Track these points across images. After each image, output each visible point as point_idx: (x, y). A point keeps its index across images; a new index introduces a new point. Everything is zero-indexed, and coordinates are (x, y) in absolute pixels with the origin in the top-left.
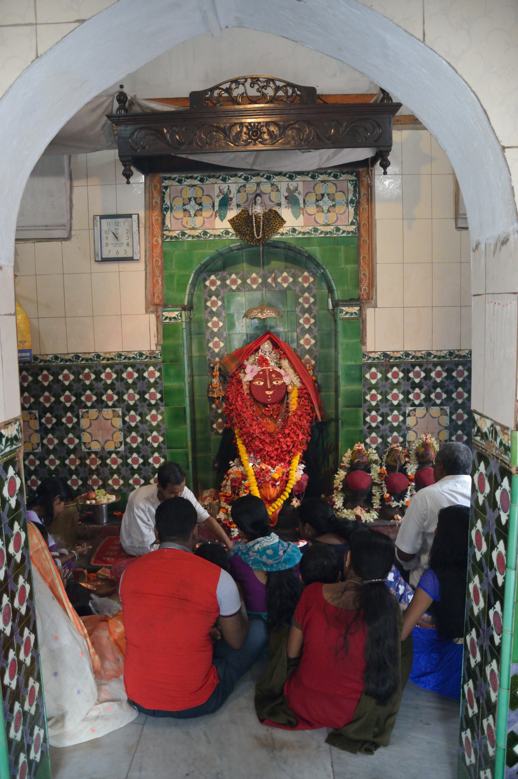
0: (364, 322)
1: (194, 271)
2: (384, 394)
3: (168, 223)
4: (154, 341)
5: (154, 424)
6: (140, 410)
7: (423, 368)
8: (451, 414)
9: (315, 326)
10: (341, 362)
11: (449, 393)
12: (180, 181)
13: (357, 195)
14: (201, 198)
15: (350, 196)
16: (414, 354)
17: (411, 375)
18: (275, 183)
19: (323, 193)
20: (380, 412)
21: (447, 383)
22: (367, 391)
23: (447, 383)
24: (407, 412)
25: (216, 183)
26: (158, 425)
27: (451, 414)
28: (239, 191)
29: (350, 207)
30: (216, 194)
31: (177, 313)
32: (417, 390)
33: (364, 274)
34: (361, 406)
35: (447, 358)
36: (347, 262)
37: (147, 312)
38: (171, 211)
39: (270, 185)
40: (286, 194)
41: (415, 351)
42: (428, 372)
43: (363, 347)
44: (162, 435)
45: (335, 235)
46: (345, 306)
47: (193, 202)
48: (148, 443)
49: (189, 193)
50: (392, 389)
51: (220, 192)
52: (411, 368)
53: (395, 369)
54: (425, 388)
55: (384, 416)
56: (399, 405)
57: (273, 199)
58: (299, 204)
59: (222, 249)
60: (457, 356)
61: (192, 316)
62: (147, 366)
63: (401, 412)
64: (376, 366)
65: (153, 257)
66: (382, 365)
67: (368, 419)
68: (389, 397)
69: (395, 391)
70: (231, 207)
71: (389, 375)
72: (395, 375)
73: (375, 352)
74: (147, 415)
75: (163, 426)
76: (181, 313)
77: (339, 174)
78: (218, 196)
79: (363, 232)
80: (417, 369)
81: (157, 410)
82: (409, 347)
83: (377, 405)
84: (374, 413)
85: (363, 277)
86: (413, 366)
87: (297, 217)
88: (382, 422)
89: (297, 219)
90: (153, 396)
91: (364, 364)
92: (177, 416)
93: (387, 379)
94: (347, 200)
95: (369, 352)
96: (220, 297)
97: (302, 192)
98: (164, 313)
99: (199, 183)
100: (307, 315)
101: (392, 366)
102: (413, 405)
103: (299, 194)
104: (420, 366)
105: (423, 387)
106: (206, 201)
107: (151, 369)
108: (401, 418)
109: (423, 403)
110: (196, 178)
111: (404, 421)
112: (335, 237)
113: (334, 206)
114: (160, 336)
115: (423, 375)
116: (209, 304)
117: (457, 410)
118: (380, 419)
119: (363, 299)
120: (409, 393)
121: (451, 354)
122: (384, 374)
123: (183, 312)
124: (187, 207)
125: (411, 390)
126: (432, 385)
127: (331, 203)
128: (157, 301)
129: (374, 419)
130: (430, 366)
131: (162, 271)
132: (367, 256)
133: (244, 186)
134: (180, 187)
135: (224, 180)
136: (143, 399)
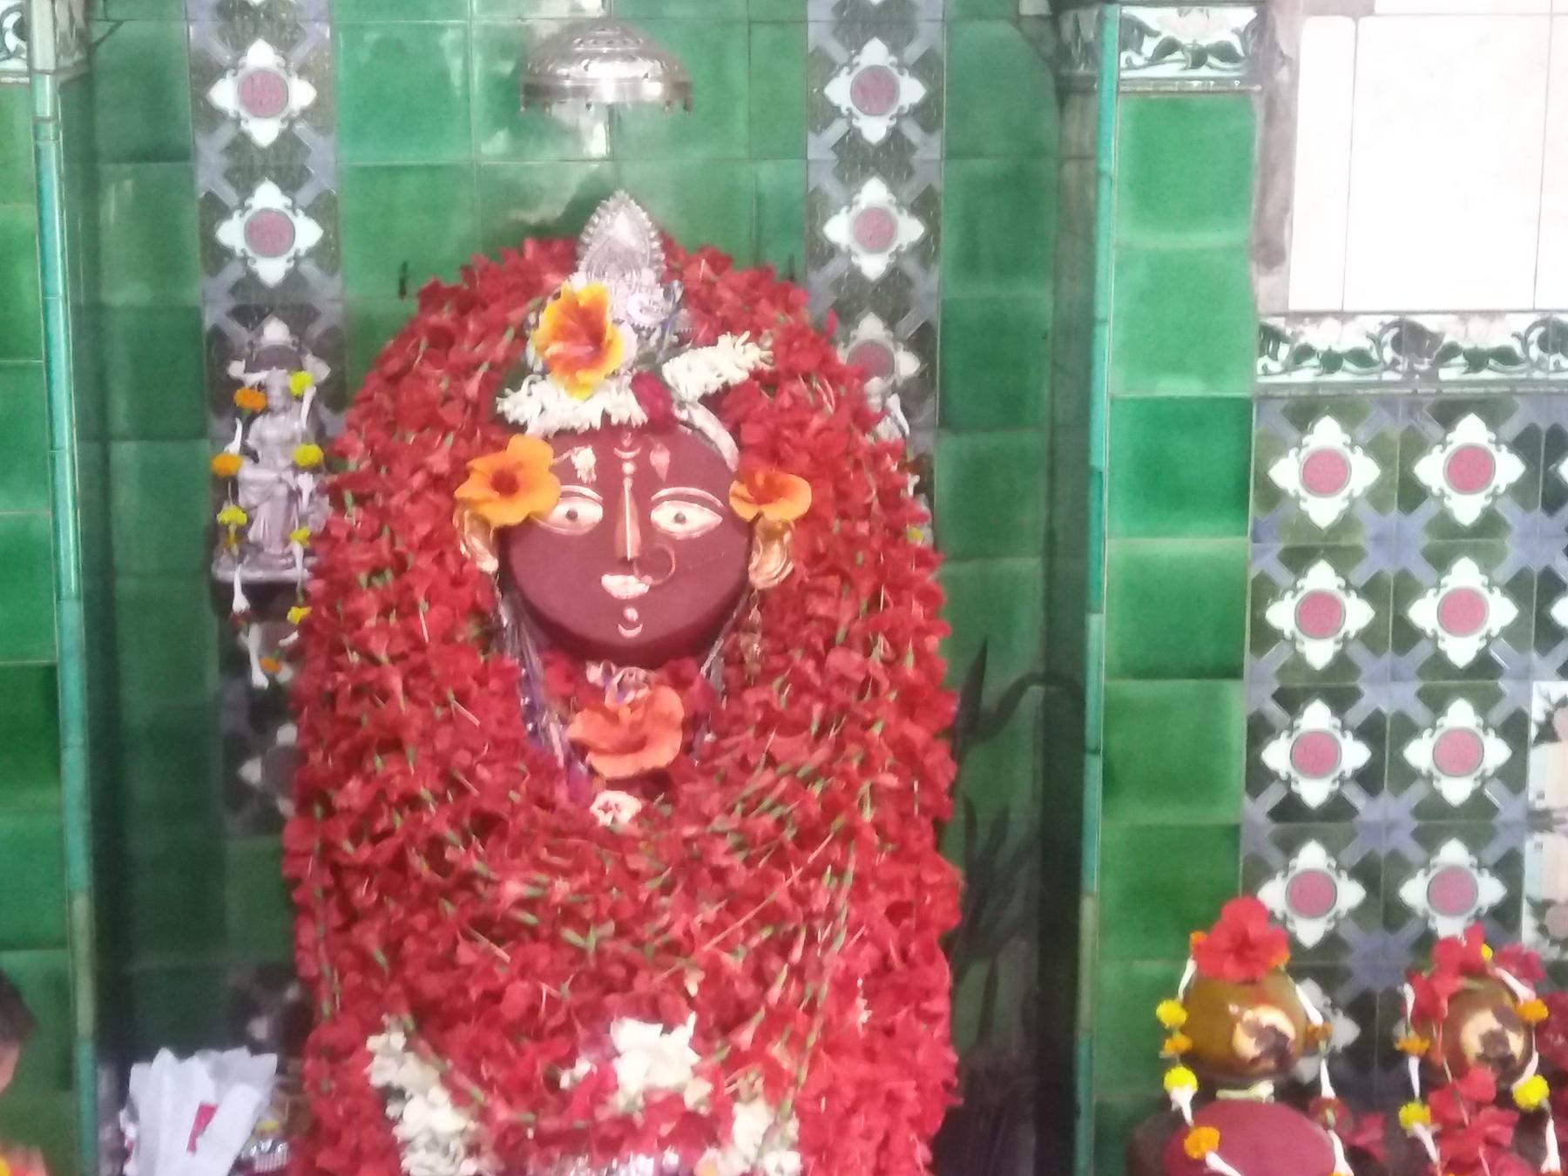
0: (1278, 111)
9: (928, 127)
10: (1113, 379)
20: (1357, 714)
22: (1281, 574)
24: (1537, 713)
34: (1235, 672)
43: (1264, 284)
50: (1440, 561)
53: (1471, 430)
56: (1484, 666)
63: (1499, 714)
64: (1347, 408)
66: (1387, 403)
67: (1277, 755)
69: (1465, 573)
71: (1431, 470)
72: (1470, 470)
73: (1342, 316)
83: (1342, 664)
84: (1317, 716)
88: (1368, 779)
91: (1266, 397)
93: (1411, 494)
95: (1300, 316)
101: (1448, 412)
108: (1496, 752)
111: (1514, 775)
118: (1355, 754)
129: (1315, 756)
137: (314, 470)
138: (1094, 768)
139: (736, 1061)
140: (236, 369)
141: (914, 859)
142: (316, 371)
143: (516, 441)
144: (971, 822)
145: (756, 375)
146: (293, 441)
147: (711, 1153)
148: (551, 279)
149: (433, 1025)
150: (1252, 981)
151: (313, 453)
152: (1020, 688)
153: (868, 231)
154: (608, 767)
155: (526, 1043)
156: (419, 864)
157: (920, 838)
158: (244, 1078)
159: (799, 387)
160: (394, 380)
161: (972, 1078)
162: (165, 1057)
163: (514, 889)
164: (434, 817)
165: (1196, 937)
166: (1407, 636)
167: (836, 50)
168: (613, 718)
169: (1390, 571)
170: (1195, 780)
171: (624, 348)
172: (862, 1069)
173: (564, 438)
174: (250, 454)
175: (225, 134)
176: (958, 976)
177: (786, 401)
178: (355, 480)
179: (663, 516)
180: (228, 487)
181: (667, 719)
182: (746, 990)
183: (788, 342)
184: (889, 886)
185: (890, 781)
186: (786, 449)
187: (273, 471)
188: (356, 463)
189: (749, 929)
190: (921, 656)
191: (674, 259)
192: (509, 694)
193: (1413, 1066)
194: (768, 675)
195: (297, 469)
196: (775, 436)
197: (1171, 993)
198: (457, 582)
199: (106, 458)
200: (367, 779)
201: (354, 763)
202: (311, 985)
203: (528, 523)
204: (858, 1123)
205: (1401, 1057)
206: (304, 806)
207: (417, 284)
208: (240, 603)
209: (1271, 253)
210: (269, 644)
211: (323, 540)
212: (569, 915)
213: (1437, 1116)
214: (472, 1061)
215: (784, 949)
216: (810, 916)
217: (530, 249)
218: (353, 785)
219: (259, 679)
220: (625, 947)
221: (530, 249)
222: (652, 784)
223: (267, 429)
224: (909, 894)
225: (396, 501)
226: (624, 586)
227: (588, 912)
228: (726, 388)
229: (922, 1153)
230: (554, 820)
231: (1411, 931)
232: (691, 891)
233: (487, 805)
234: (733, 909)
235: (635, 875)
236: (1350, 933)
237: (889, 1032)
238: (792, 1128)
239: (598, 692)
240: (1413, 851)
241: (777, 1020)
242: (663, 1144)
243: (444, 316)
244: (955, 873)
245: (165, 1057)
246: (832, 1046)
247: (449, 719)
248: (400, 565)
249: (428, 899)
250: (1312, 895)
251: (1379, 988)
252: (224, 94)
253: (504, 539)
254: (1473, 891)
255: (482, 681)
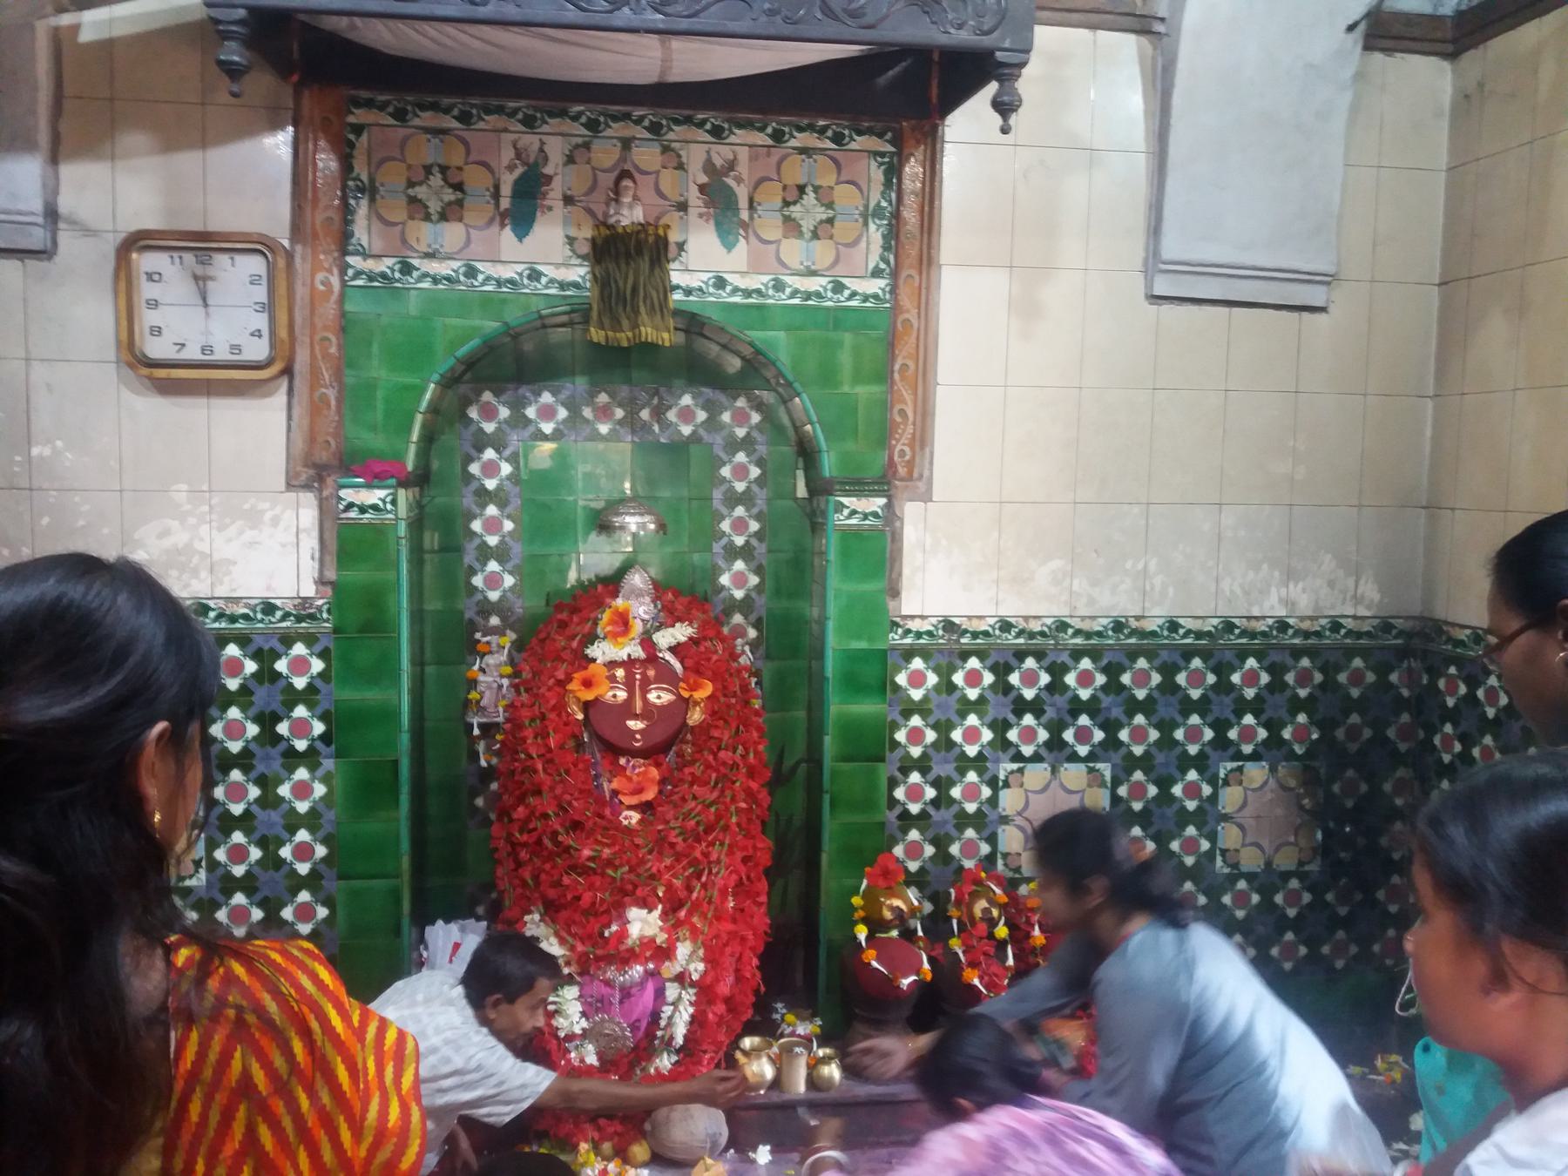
0: (897, 537)
1: (436, 377)
2: (943, 728)
3: (361, 232)
4: (310, 569)
5: (302, 807)
6: (261, 768)
7: (1046, 662)
8: (1116, 782)
10: (833, 641)
11: (1111, 727)
12: (401, 115)
13: (893, 195)
14: (460, 169)
15: (875, 197)
16: (1022, 624)
17: (1014, 679)
18: (674, 145)
19: (801, 181)
20: (932, 776)
21: (1106, 701)
22: (900, 719)
23: (1106, 701)
24: (1002, 777)
25: (506, 130)
26: (313, 812)
27: (1116, 782)
28: (570, 160)
29: (872, 227)
30: (505, 161)
31: (382, 493)
32: (1028, 719)
33: (902, 412)
34: (882, 760)
35: (1108, 637)
36: (858, 378)
37: (290, 486)
38: (372, 200)
39: (658, 150)
40: (703, 179)
41: (1026, 618)
42: (1057, 671)
43: (892, 604)
44: (325, 841)
45: (830, 304)
46: (848, 494)
47: (436, 180)
48: (280, 863)
49: (428, 151)
50: (963, 715)
51: (518, 155)
52: (1013, 662)
53: (973, 663)
54: (1050, 713)
55: (942, 785)
56: (980, 756)
57: (665, 187)
58: (736, 210)
59: (514, 316)
60: (1134, 632)
61: (425, 501)
62: (288, 640)
63: (987, 776)
64: (925, 653)
65: (313, 326)
66: (941, 651)
67: (899, 793)
68: (957, 735)
69: (972, 720)
70: (547, 202)
71: (958, 678)
72: (973, 678)
73: (923, 617)
74: (281, 782)
75: (330, 815)
76: (395, 496)
77: (846, 132)
78: (511, 168)
79: (906, 301)
80: (1030, 663)
81: (313, 768)
82: (1013, 607)
83: (924, 755)
84: (915, 777)
85: (898, 419)
86: (1020, 655)
87: (729, 246)
88: (935, 803)
89: (729, 251)
90: (301, 728)
91: (894, 648)
92: (369, 787)
93: (952, 688)
94: (866, 207)
96: (507, 452)
97: (745, 176)
98: (342, 493)
99: (455, 124)
100: (740, 511)
101: (965, 655)
102: (1018, 757)
103: (739, 180)
104: (1039, 655)
105: (1044, 712)
106: (476, 180)
107: (299, 649)
108: (986, 792)
109: (1044, 752)
110: (447, 111)
111: (993, 801)
112: (828, 309)
113: (830, 221)
114: (331, 560)
115: (1045, 679)
116: (474, 468)
117: (1130, 773)
118: (930, 793)
119: (892, 473)
120: (1007, 725)
121: (1118, 626)
122: (945, 673)
123: (402, 493)
124: (421, 192)
125: (1012, 718)
126: (1067, 707)
127: (821, 214)
128: (323, 456)
129: (915, 793)
130: (1065, 658)
131: (338, 375)
132: (911, 364)
133: (587, 146)
134: (402, 132)
135: (529, 122)
136: (269, 736)
137: (509, 677)
138: (827, 798)
139: (678, 924)
140: (478, 635)
141: (753, 837)
142: (512, 635)
143: (592, 666)
144: (777, 821)
145: (691, 639)
146: (500, 665)
147: (667, 963)
148: (608, 600)
149: (552, 911)
150: (889, 888)
151: (508, 670)
152: (794, 769)
153: (736, 580)
154: (627, 800)
155: (592, 919)
156: (547, 843)
157: (756, 828)
158: (473, 932)
159: (708, 644)
160: (543, 641)
161: (777, 928)
162: (440, 923)
163: (587, 853)
164: (555, 824)
165: (867, 869)
166: (951, 744)
167: (724, 511)
168: (630, 779)
169: (943, 718)
170: (868, 804)
171: (637, 628)
172: (731, 927)
173: (612, 665)
174: (482, 670)
175: (477, 542)
176: (771, 885)
177: (702, 649)
178: (524, 682)
179: (652, 697)
180: (473, 684)
181: (652, 780)
182: (682, 894)
183: (703, 627)
184: (745, 848)
185: (743, 805)
186: (702, 669)
187: (492, 675)
188: (526, 675)
189: (684, 869)
190: (756, 753)
191: (659, 589)
192: (587, 770)
193: (955, 922)
194: (692, 763)
195: (502, 676)
196: (698, 663)
197: (856, 892)
198: (566, 724)
199: (422, 672)
200: (527, 806)
201: (521, 800)
202: (502, 893)
203: (596, 699)
204: (728, 950)
205: (949, 919)
206: (500, 819)
207: (555, 601)
208: (476, 732)
209: (895, 593)
210: (488, 749)
211: (510, 707)
212: (609, 863)
213: (964, 944)
214: (568, 925)
215: (699, 877)
216: (710, 863)
217: (600, 588)
218: (521, 809)
219: (483, 763)
220: (632, 877)
221: (600, 588)
222: (644, 807)
223: (490, 660)
224: (751, 852)
225: (543, 690)
226: (635, 725)
227: (617, 862)
228: (679, 644)
229: (755, 962)
230: (604, 823)
231: (954, 866)
232: (660, 853)
233: (577, 818)
234: (678, 860)
235: (637, 846)
236: (929, 866)
237: (742, 910)
238: (701, 952)
239: (624, 768)
240: (954, 832)
241: (696, 907)
242: (647, 960)
243: (564, 616)
244: (770, 843)
245: (440, 923)
246: (718, 918)
247: (561, 781)
248: (543, 717)
249: (551, 857)
250: (914, 851)
251: (941, 889)
252: (476, 526)
253: (586, 706)
254: (978, 849)
255: (575, 766)
